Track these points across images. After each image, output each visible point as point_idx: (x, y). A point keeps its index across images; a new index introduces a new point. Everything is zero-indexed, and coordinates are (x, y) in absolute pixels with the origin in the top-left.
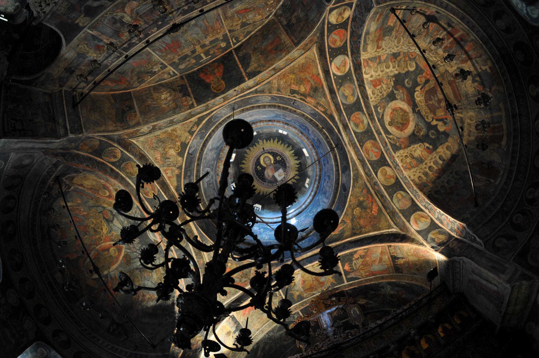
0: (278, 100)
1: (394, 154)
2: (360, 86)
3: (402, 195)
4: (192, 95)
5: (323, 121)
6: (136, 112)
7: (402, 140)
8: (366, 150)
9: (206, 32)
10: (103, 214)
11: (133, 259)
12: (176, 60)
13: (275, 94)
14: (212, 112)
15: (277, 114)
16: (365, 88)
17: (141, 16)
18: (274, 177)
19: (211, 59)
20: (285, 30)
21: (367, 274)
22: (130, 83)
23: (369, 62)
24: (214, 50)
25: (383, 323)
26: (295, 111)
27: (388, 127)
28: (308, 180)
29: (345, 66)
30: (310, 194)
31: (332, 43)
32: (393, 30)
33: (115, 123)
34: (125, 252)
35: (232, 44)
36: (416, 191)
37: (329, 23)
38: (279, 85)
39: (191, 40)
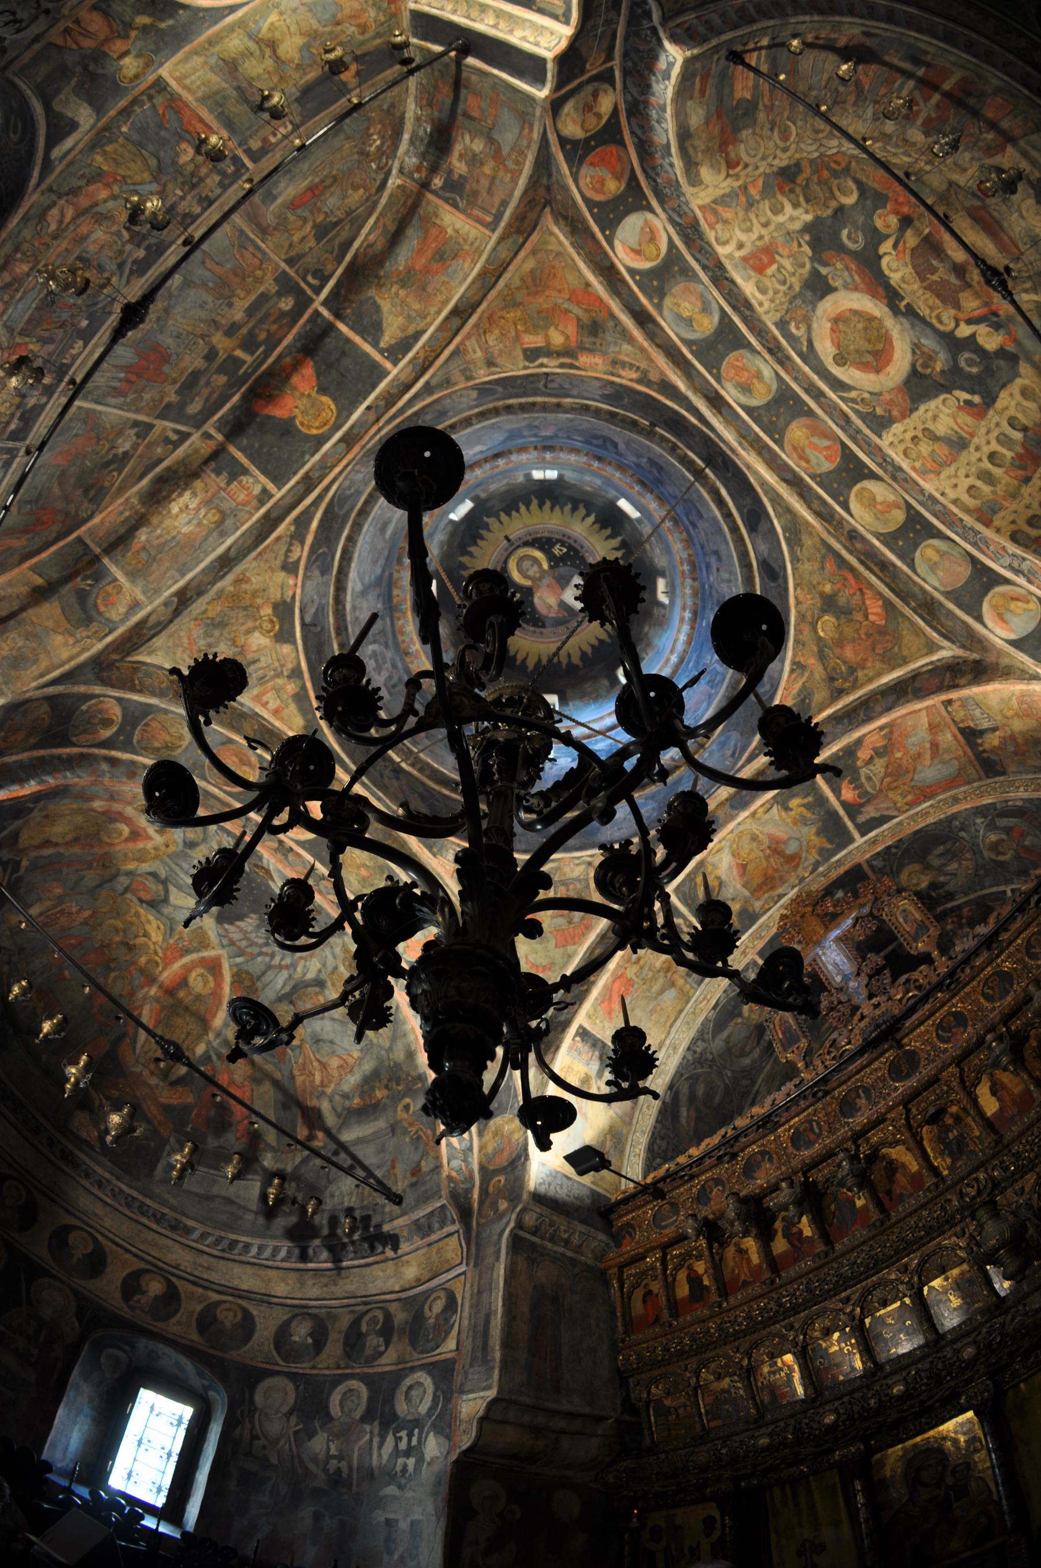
0: (500, 389)
1: (878, 441)
2: (715, 280)
3: (938, 551)
5: (647, 405)
6: (116, 580)
7: (887, 397)
8: (795, 448)
9: (224, 291)
12: (172, 398)
13: (483, 376)
15: (511, 431)
16: (733, 282)
17: (23, 333)
19: (266, 355)
20: (447, 200)
21: (909, 798)
23: (720, 209)
25: (996, 933)
26: (558, 405)
28: (661, 584)
29: (653, 239)
30: (682, 619)
31: (594, 189)
32: (756, 107)
33: (72, 635)
35: (309, 292)
36: (972, 529)
37: (563, 141)
38: (486, 350)
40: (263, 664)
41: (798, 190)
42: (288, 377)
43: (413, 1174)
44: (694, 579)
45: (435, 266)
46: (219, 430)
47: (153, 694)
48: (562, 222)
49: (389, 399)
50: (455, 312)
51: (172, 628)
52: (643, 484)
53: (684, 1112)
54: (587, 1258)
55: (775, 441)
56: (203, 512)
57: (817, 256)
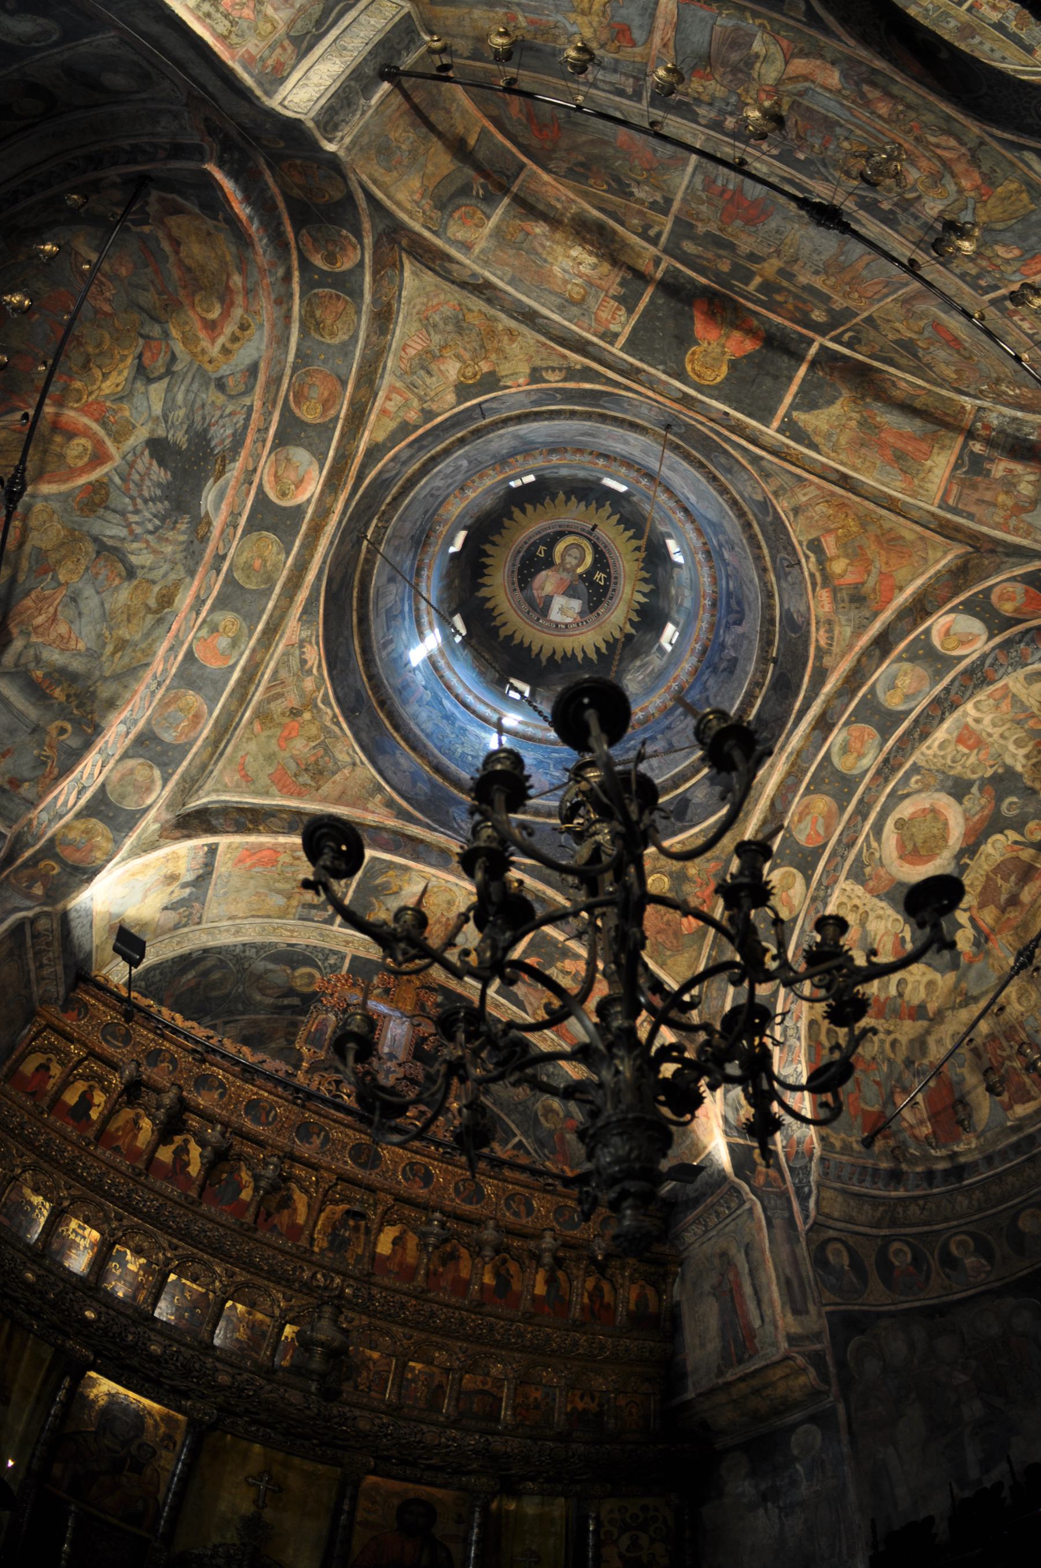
0: (769, 519)
2: (937, 701)
4: (635, 317)
7: (882, 872)
11: (107, 508)
13: (782, 506)
14: (627, 388)
18: (548, 600)
20: (960, 457)
22: (553, 151)
23: (1009, 700)
38: (808, 505)
39: (788, 241)
40: (428, 381)
42: (738, 328)
43: (11, 782)
45: (889, 452)
46: (666, 272)
47: (374, 294)
48: (959, 562)
49: (738, 429)
50: (845, 477)
52: (704, 651)
53: (191, 974)
54: (37, 992)
55: (807, 788)
56: (578, 281)
57: (984, 782)
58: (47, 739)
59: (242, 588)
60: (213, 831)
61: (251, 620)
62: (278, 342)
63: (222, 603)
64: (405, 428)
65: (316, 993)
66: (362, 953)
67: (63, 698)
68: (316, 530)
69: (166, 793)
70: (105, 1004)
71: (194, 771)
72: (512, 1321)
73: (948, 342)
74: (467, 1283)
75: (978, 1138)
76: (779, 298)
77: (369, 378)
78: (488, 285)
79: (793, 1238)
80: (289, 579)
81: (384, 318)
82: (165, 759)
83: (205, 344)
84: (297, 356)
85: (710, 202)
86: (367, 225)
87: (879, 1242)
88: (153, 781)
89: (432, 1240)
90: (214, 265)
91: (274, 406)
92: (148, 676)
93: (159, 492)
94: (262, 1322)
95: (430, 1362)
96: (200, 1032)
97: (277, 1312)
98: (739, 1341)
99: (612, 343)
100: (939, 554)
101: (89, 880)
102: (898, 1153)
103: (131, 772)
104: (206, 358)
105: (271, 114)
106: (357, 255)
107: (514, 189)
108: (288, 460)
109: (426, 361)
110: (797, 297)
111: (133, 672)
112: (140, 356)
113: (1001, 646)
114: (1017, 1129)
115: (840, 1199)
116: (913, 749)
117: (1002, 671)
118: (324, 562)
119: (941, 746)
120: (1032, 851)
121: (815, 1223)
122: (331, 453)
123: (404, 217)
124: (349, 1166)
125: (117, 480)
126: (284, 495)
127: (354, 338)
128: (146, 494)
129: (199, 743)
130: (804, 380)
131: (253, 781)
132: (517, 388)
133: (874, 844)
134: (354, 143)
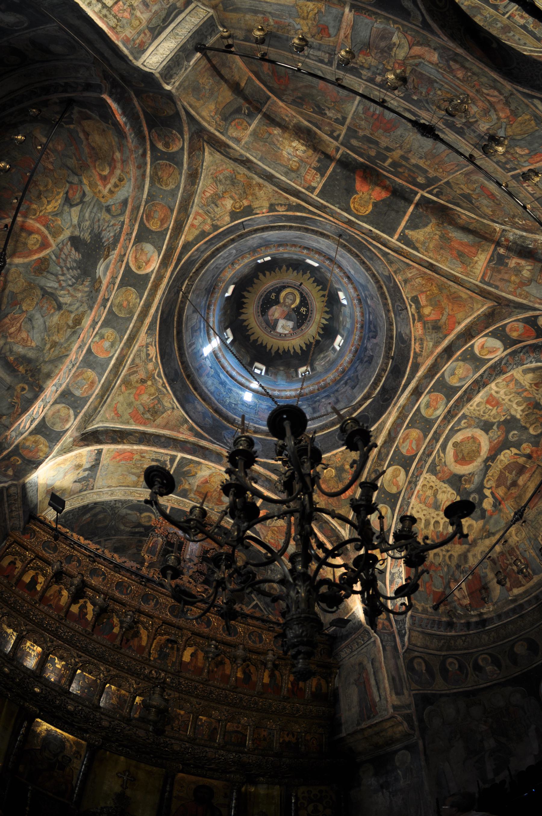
0: (392, 285)
2: (476, 382)
4: (325, 179)
7: (446, 469)
10: (71, 187)
11: (48, 272)
13: (398, 279)
14: (319, 216)
15: (367, 287)
20: (492, 256)
23: (514, 382)
24: (407, 171)
27: (450, 444)
34: (48, 254)
35: (428, 189)
38: (412, 278)
40: (216, 210)
41: (530, 411)
42: (378, 185)
44: (318, 389)
45: (455, 252)
47: (189, 164)
48: (490, 310)
49: (377, 238)
50: (431, 265)
51: (227, 160)
53: (88, 515)
54: (9, 524)
57: (500, 424)
58: (15, 394)
59: (116, 316)
60: (100, 442)
61: (122, 333)
62: (138, 188)
63: (106, 323)
64: (203, 234)
65: (151, 526)
66: (176, 506)
67: (23, 372)
68: (156, 287)
69: (76, 422)
70: (44, 531)
71: (90, 411)
72: (252, 696)
73: (488, 196)
74: (229, 677)
75: (494, 605)
76: (400, 170)
77: (185, 208)
78: (248, 161)
79: (396, 656)
80: (141, 312)
81: (194, 177)
82: (76, 405)
83: (101, 188)
84: (148, 195)
85: (366, 120)
86: (186, 129)
87: (441, 658)
88: (69, 416)
89: (211, 655)
90: (106, 147)
91: (135, 221)
92: (67, 361)
93: (75, 265)
94: (124, 695)
95: (210, 716)
96: (93, 546)
97: (132, 690)
98: (368, 708)
99: (312, 193)
100: (480, 306)
101: (37, 467)
102: (451, 613)
103: (58, 411)
104: (101, 195)
105: (137, 69)
106: (181, 144)
107: (264, 110)
108: (142, 250)
109: (215, 200)
110: (410, 170)
111: (60, 359)
112: (67, 193)
113: (511, 354)
114: (514, 601)
115: (421, 636)
116: (463, 406)
117: (510, 367)
118: (160, 303)
119: (478, 405)
120: (524, 459)
121: (408, 649)
122: (165, 247)
123: (205, 124)
124: (169, 617)
125: (54, 257)
126: (139, 268)
127: (178, 187)
128: (68, 265)
129: (93, 397)
130: (412, 213)
131: (121, 417)
132: (262, 214)
133: (442, 455)
134: (180, 85)
